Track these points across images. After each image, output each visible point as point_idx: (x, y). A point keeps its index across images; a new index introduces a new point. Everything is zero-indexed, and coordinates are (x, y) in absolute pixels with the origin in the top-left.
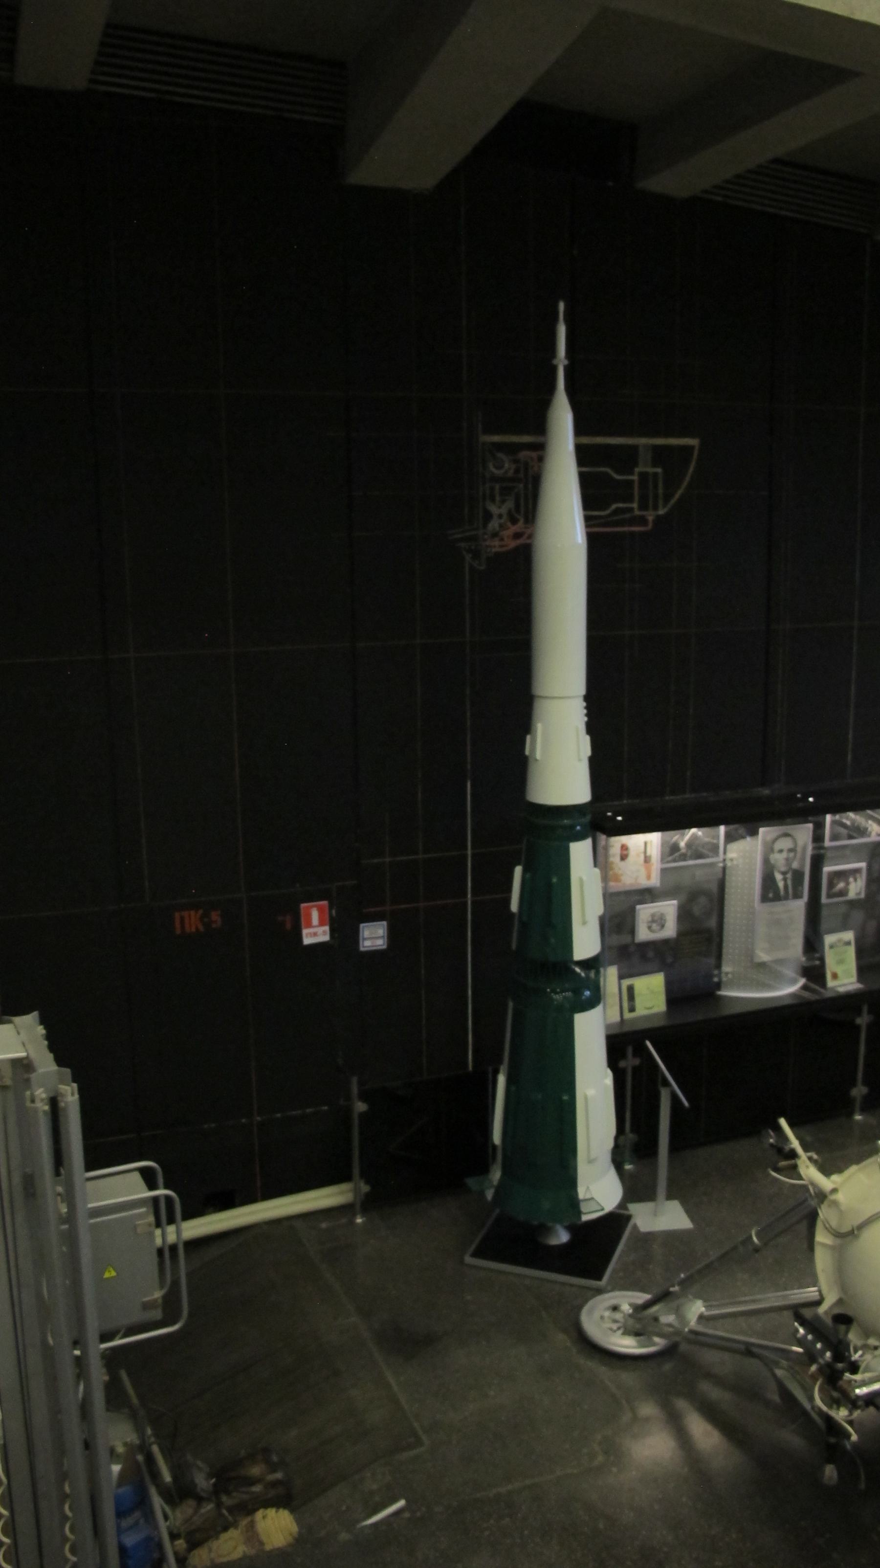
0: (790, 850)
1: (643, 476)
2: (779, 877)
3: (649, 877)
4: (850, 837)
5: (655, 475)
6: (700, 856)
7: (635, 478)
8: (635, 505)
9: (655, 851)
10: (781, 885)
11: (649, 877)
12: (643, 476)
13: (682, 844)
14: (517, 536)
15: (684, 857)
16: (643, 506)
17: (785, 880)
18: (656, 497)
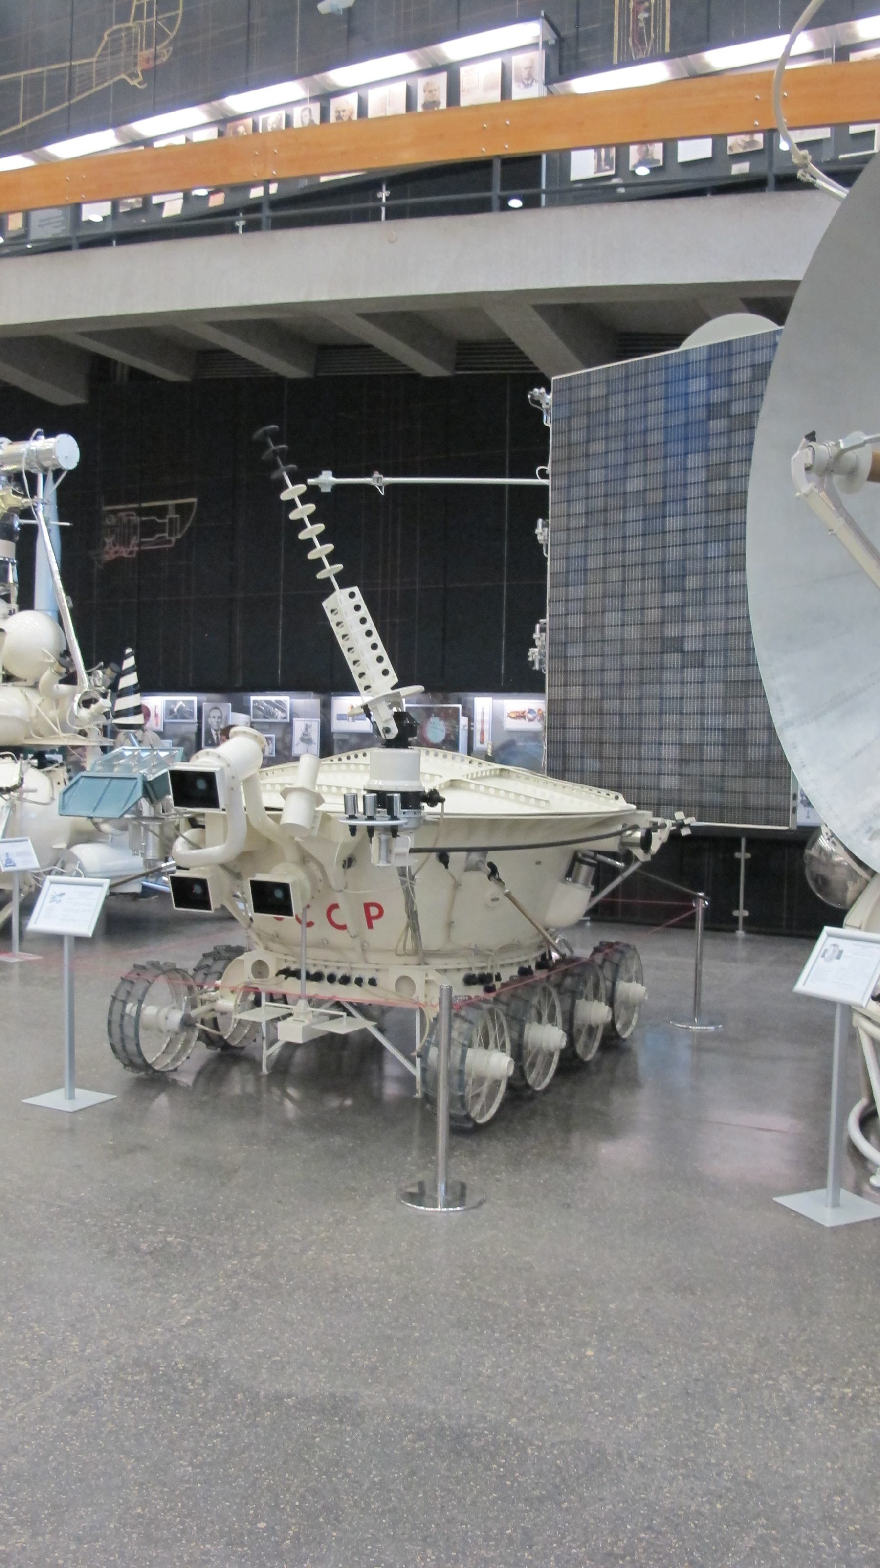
0: (219, 717)
1: (171, 520)
2: (213, 732)
3: (157, 725)
4: (265, 717)
5: (176, 519)
6: (184, 718)
7: (167, 521)
8: (166, 534)
9: (161, 711)
10: (215, 737)
11: (157, 725)
12: (171, 520)
13: (175, 710)
14: (116, 552)
15: (176, 717)
16: (170, 534)
17: (217, 734)
18: (176, 529)
